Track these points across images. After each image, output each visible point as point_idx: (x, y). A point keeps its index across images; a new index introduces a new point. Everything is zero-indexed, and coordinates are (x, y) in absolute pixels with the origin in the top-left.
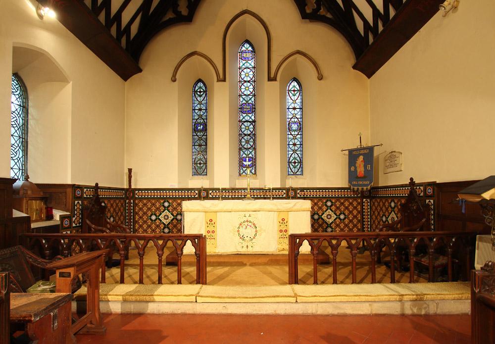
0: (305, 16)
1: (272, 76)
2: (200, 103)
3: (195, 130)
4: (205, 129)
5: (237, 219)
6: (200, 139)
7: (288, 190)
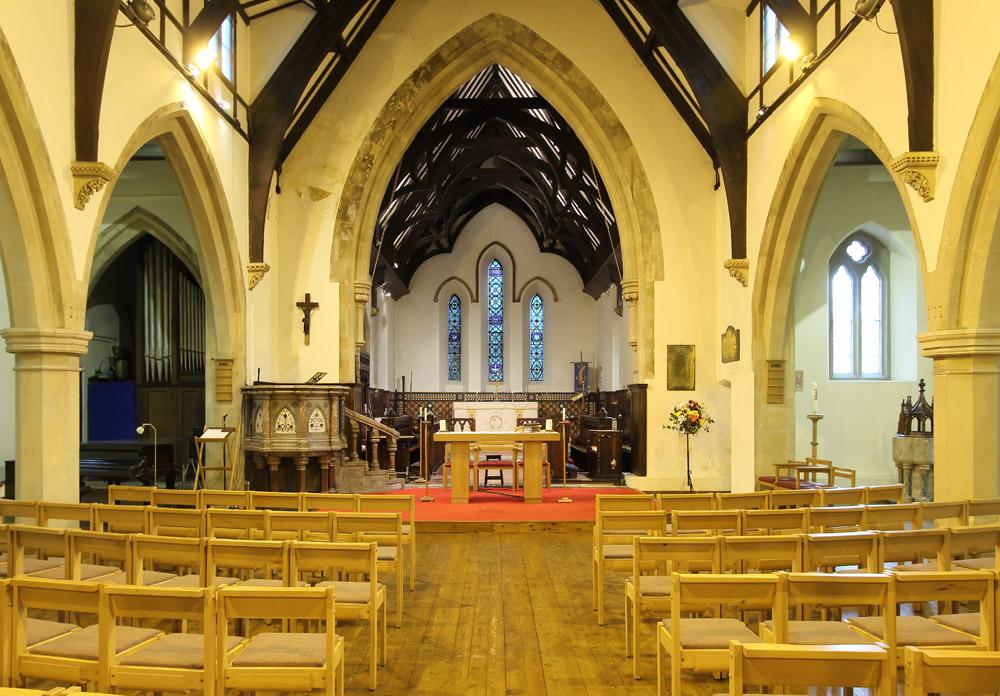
0: (543, 250)
1: (516, 298)
2: (455, 315)
3: (450, 339)
4: (459, 339)
5: (490, 414)
6: (455, 347)
7: (529, 394)
